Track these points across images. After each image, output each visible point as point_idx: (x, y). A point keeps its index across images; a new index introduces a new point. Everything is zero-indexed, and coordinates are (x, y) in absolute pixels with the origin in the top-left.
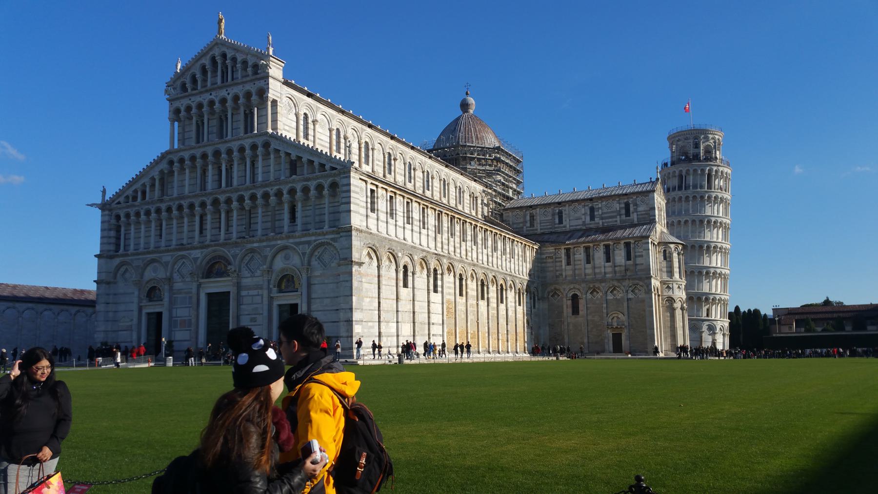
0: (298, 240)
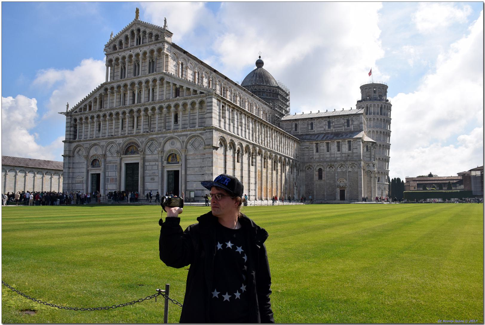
0: (180, 134)
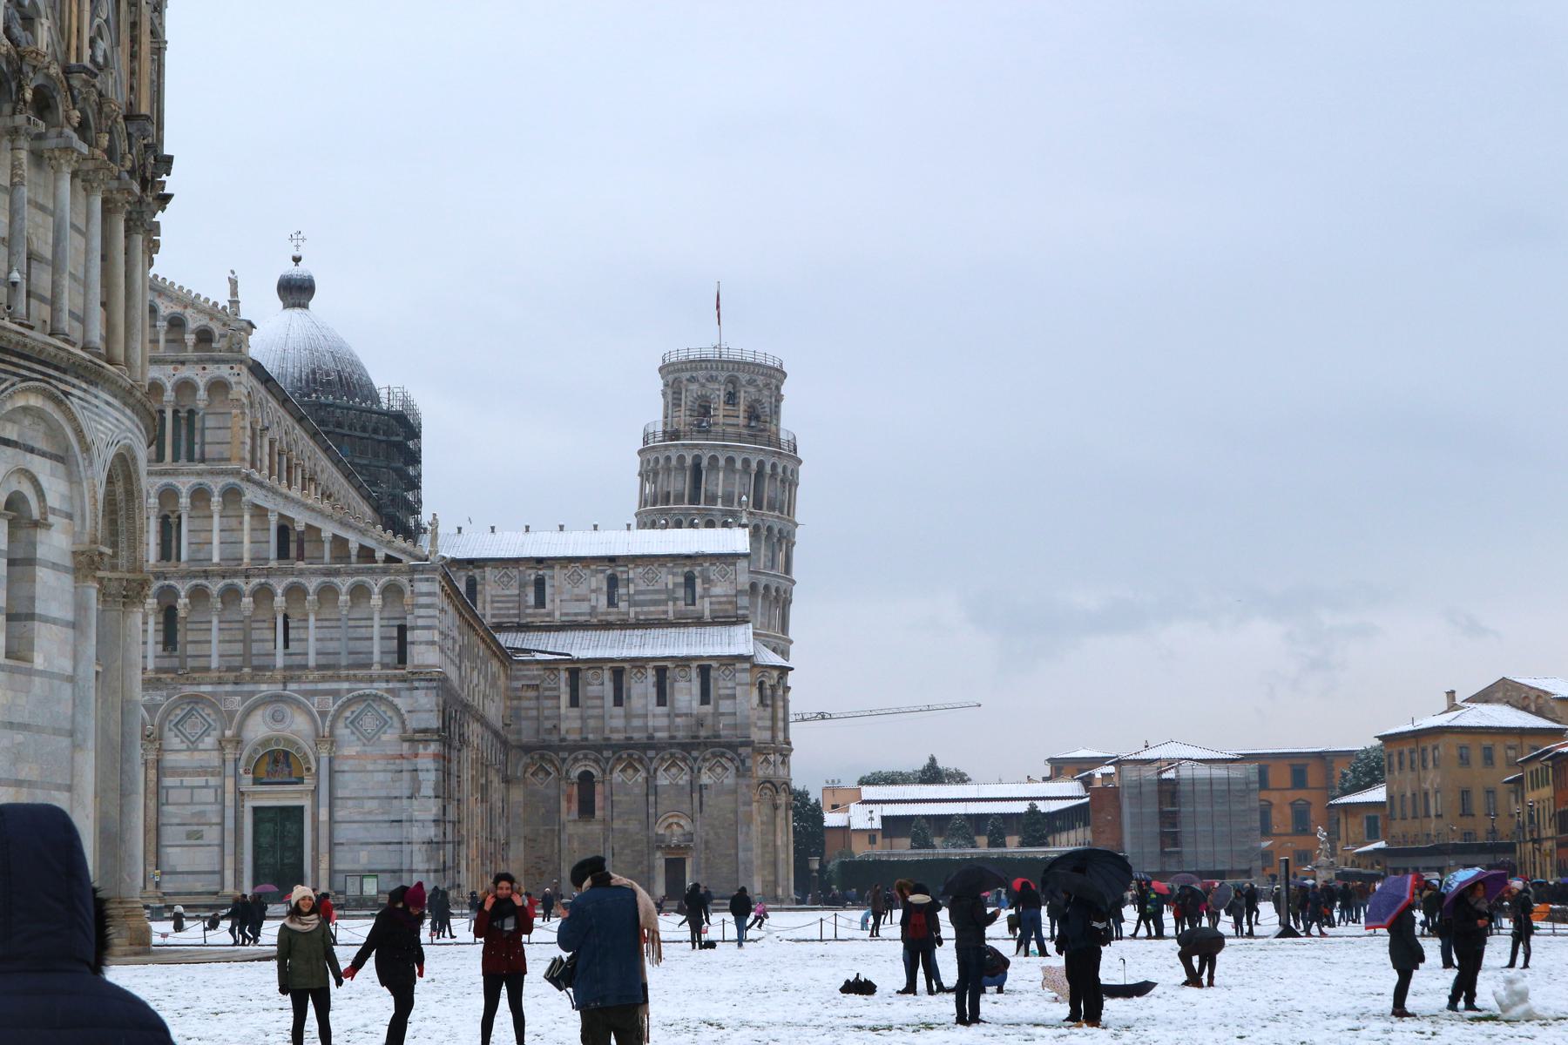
0: (304, 687)
